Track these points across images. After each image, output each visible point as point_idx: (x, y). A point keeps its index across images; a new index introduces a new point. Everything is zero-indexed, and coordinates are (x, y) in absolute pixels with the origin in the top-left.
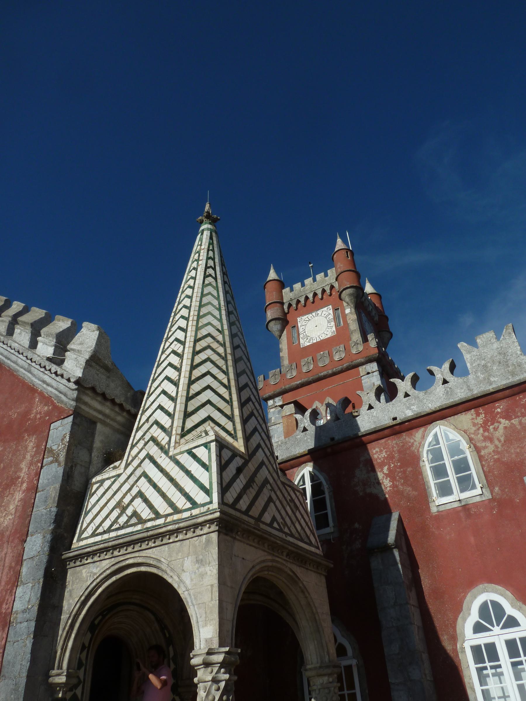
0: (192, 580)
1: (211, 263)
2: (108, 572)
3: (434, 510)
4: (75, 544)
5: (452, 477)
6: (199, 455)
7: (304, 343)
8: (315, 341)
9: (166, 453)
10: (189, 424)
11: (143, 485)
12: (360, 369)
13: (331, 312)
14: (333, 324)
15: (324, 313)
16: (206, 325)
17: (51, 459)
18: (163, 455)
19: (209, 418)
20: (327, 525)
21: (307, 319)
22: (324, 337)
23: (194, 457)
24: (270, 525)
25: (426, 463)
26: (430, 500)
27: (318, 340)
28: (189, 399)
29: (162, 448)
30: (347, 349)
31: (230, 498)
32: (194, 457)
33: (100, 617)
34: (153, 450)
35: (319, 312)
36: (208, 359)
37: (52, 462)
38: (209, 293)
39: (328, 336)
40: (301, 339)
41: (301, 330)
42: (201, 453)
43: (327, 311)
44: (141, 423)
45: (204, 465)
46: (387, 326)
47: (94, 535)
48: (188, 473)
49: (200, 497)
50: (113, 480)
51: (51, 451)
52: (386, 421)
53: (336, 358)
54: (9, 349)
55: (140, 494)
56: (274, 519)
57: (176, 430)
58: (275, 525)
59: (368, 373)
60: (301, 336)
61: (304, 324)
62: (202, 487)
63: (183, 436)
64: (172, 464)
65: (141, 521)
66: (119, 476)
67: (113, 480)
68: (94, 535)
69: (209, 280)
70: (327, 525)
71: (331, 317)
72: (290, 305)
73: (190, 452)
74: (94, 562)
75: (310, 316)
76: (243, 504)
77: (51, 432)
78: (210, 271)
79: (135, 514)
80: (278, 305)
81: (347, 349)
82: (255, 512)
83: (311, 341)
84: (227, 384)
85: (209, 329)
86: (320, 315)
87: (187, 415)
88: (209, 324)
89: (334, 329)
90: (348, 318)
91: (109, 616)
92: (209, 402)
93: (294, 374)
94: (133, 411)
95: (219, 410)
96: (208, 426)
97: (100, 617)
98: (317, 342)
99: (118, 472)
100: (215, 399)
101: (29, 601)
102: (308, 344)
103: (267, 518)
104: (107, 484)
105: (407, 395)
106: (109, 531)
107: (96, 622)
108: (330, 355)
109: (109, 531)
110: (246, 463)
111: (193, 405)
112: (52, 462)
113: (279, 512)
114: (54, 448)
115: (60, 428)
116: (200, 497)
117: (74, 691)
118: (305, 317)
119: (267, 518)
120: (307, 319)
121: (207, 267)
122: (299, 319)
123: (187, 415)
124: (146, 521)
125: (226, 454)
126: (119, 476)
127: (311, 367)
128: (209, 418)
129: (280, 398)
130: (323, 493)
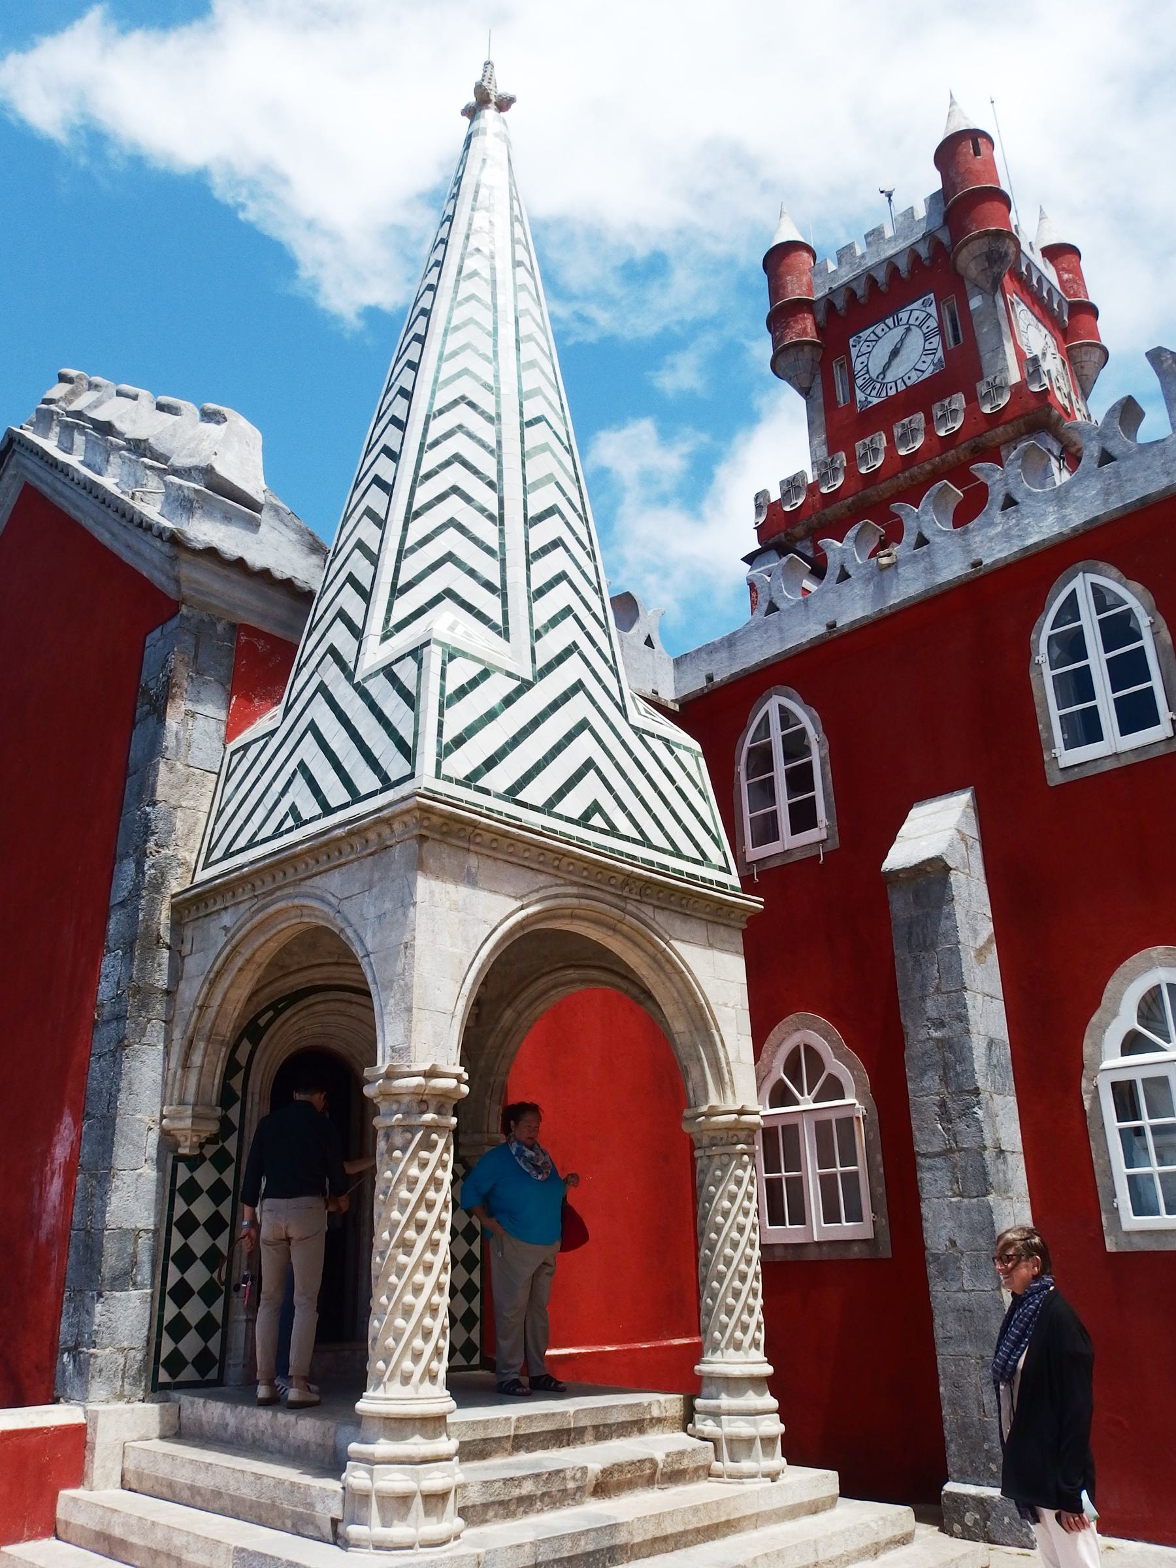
0: (374, 935)
2: (248, 926)
3: (1055, 779)
5: (1105, 700)
6: (402, 676)
8: (892, 392)
11: (309, 751)
13: (933, 310)
14: (936, 340)
15: (916, 314)
16: (459, 375)
17: (146, 708)
18: (345, 683)
20: (813, 823)
21: (873, 337)
22: (915, 378)
24: (583, 820)
25: (1046, 668)
26: (1046, 758)
27: (901, 387)
28: (401, 555)
31: (461, 763)
33: (270, 1014)
34: (332, 674)
35: (904, 315)
37: (148, 714)
39: (926, 375)
40: (858, 391)
41: (858, 367)
42: (406, 672)
43: (921, 313)
44: (317, 618)
50: (262, 743)
54: (72, 485)
56: (595, 807)
57: (375, 627)
58: (597, 820)
60: (859, 382)
61: (864, 349)
63: (385, 638)
64: (359, 702)
66: (272, 733)
67: (262, 743)
68: (228, 855)
70: (814, 824)
71: (933, 323)
74: (226, 908)
75: (879, 329)
76: (500, 779)
77: (146, 653)
83: (884, 394)
84: (496, 513)
86: (904, 321)
87: (397, 591)
88: (465, 372)
89: (940, 354)
90: (976, 320)
91: (288, 1013)
92: (450, 557)
95: (472, 573)
96: (447, 611)
97: (270, 1014)
101: (119, 983)
102: (876, 401)
103: (573, 805)
105: (1010, 502)
106: (251, 844)
107: (262, 1022)
109: (251, 844)
110: (525, 686)
112: (148, 714)
113: (610, 789)
114: (151, 684)
115: (160, 643)
116: (396, 766)
117: (221, 1144)
118: (864, 335)
119: (573, 805)
120: (873, 337)
122: (851, 341)
124: (306, 822)
126: (272, 733)
128: (449, 593)
130: (807, 751)
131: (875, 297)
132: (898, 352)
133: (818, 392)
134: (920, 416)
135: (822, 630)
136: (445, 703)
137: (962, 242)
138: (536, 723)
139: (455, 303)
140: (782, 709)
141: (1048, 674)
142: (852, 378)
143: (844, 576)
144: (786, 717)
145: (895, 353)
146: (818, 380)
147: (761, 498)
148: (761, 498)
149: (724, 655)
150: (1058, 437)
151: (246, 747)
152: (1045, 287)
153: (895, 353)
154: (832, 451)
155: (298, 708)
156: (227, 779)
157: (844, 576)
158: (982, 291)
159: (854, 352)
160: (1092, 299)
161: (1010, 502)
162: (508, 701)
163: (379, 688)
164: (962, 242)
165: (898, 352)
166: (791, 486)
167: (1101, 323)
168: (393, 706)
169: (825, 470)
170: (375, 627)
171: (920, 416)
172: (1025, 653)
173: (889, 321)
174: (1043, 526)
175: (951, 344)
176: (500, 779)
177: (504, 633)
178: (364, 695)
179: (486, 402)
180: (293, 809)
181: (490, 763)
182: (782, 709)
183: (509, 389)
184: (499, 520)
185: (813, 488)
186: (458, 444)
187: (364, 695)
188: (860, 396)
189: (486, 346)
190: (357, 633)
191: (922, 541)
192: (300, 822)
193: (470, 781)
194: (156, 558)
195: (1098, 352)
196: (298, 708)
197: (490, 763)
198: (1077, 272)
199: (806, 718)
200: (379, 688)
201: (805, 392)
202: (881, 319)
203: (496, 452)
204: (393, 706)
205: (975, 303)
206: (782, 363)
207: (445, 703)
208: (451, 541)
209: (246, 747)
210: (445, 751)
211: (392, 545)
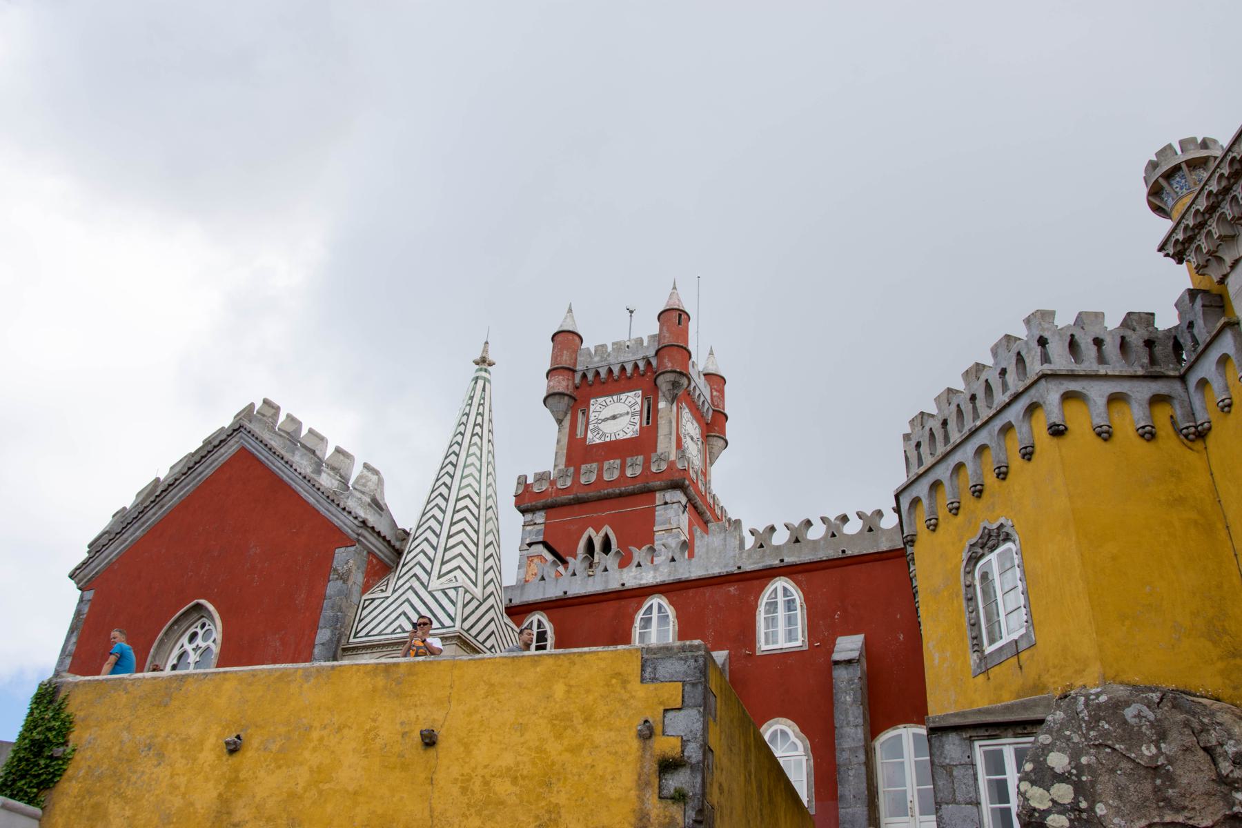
1: (479, 418)
4: (351, 640)
7: (593, 438)
9: (426, 588)
10: (445, 568)
12: (658, 495)
14: (638, 418)
19: (459, 567)
22: (622, 436)
23: (446, 594)
27: (613, 439)
28: (446, 550)
29: (422, 583)
30: (647, 462)
31: (467, 625)
32: (446, 594)
34: (416, 585)
35: (623, 397)
36: (465, 519)
38: (472, 464)
41: (592, 418)
42: (452, 593)
43: (631, 401)
45: (452, 602)
46: (723, 431)
47: (367, 635)
48: (441, 605)
49: (447, 622)
51: (336, 570)
52: (614, 585)
53: (629, 473)
55: (404, 613)
56: (493, 646)
57: (435, 573)
59: (666, 503)
60: (591, 427)
62: (449, 616)
65: (404, 631)
68: (367, 635)
69: (476, 439)
71: (638, 408)
72: (584, 376)
73: (444, 591)
75: (608, 399)
76: (474, 632)
78: (478, 429)
79: (400, 626)
80: (566, 372)
81: (647, 462)
82: (481, 638)
85: (469, 491)
87: (443, 563)
89: (638, 427)
92: (460, 555)
93: (569, 483)
94: (398, 545)
96: (458, 573)
98: (611, 442)
99: (384, 595)
100: (466, 553)
102: (598, 441)
103: (488, 644)
104: (377, 602)
105: (639, 565)
108: (623, 468)
111: (448, 555)
116: (447, 622)
118: (600, 400)
119: (488, 644)
121: (475, 425)
123: (443, 563)
125: (468, 597)
127: (593, 478)
129: (543, 513)
131: (611, 381)
132: (615, 417)
133: (567, 423)
134: (618, 461)
135: (561, 594)
136: (465, 606)
137: (662, 370)
138: (421, 600)
139: (468, 456)
140: (539, 621)
141: (638, 631)
142: (587, 424)
143: (574, 574)
144: (540, 624)
145: (614, 417)
146: (569, 417)
147: (522, 480)
148: (522, 480)
149: (519, 592)
150: (686, 494)
151: (373, 600)
152: (702, 399)
153: (614, 417)
154: (568, 464)
155: (400, 591)
156: (364, 608)
157: (574, 574)
158: (667, 400)
159: (592, 408)
160: (726, 411)
161: (639, 565)
162: (477, 608)
163: (439, 595)
164: (662, 370)
165: (615, 417)
166: (541, 477)
167: (728, 424)
168: (445, 602)
169: (563, 475)
170: (435, 573)
171: (618, 461)
172: (632, 622)
173: (615, 397)
174: (648, 577)
175: (644, 424)
176: (474, 632)
177: (476, 585)
178: (433, 596)
179: (476, 499)
180: (400, 626)
181: (472, 627)
182: (539, 621)
183: (483, 495)
184: (477, 545)
185: (553, 483)
186: (465, 513)
187: (433, 596)
188: (590, 435)
189: (477, 475)
190: (429, 574)
191: (606, 570)
192: (404, 631)
193: (467, 631)
194: (349, 523)
195: (722, 443)
196: (400, 591)
197: (472, 627)
198: (722, 392)
199: (548, 627)
200: (439, 595)
201: (560, 422)
202: (611, 395)
203: (478, 519)
204: (445, 602)
205: (662, 405)
206: (550, 400)
207: (465, 606)
208: (461, 549)
209: (373, 600)
210: (464, 620)
211: (442, 546)
